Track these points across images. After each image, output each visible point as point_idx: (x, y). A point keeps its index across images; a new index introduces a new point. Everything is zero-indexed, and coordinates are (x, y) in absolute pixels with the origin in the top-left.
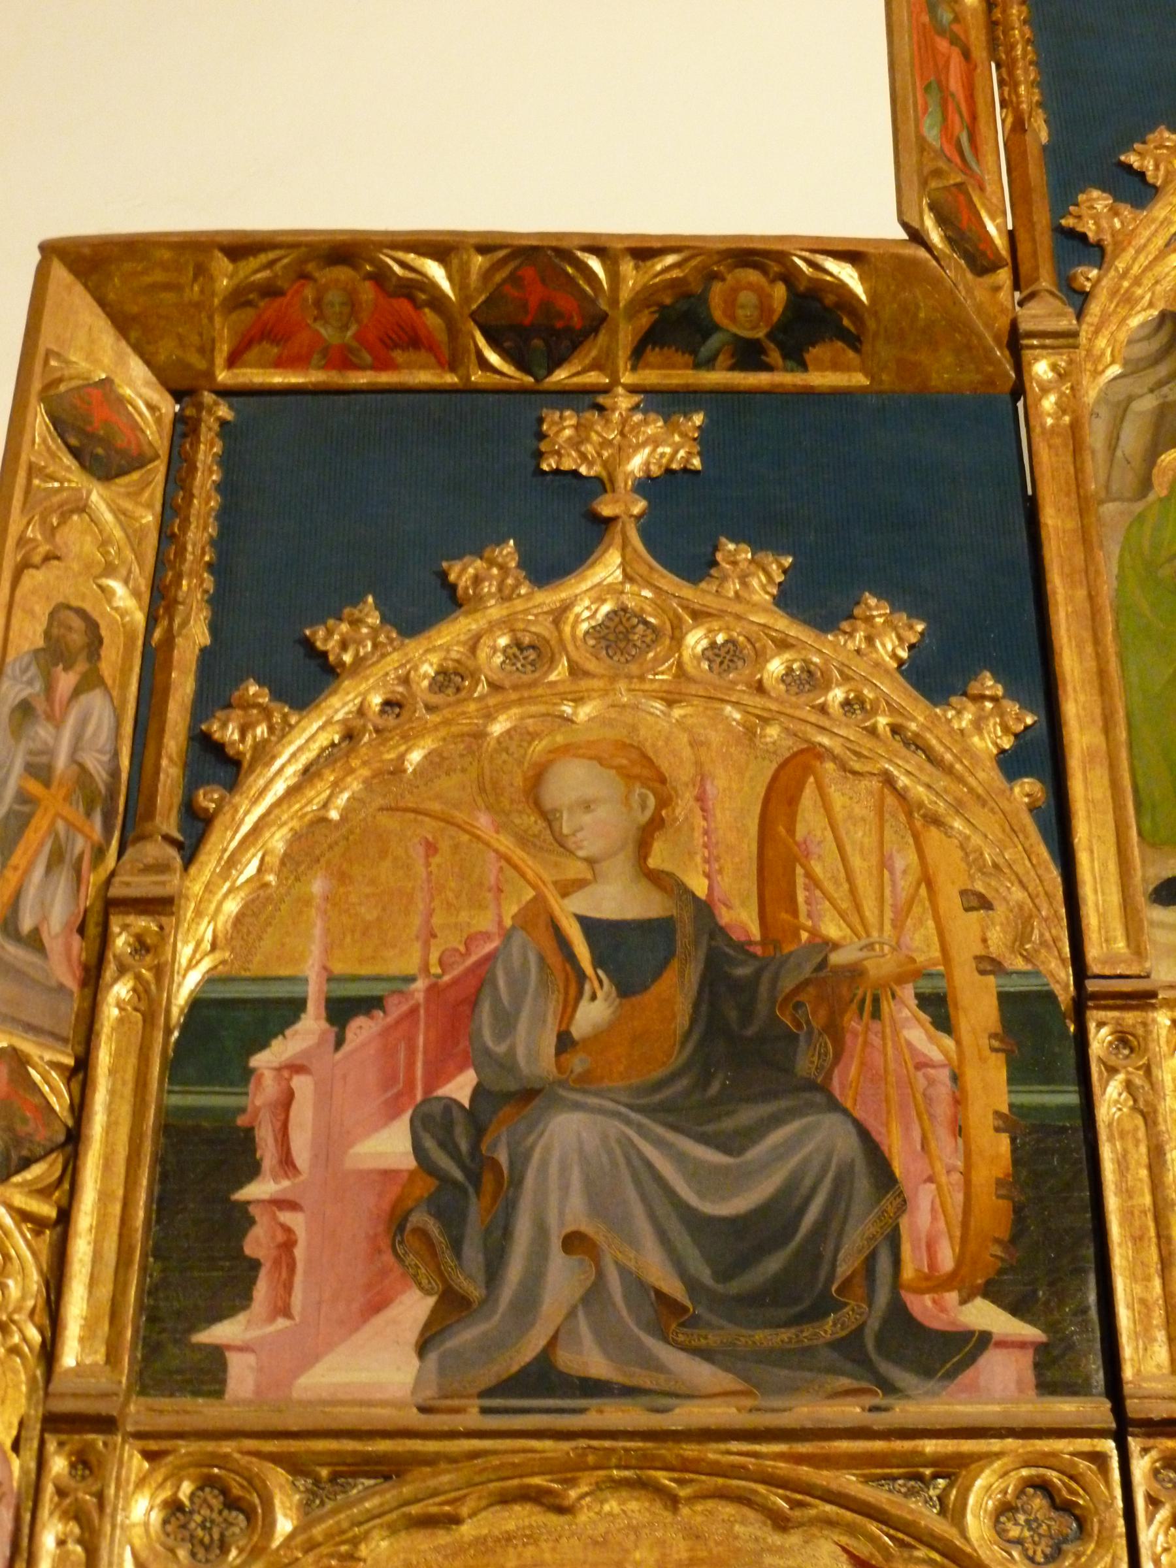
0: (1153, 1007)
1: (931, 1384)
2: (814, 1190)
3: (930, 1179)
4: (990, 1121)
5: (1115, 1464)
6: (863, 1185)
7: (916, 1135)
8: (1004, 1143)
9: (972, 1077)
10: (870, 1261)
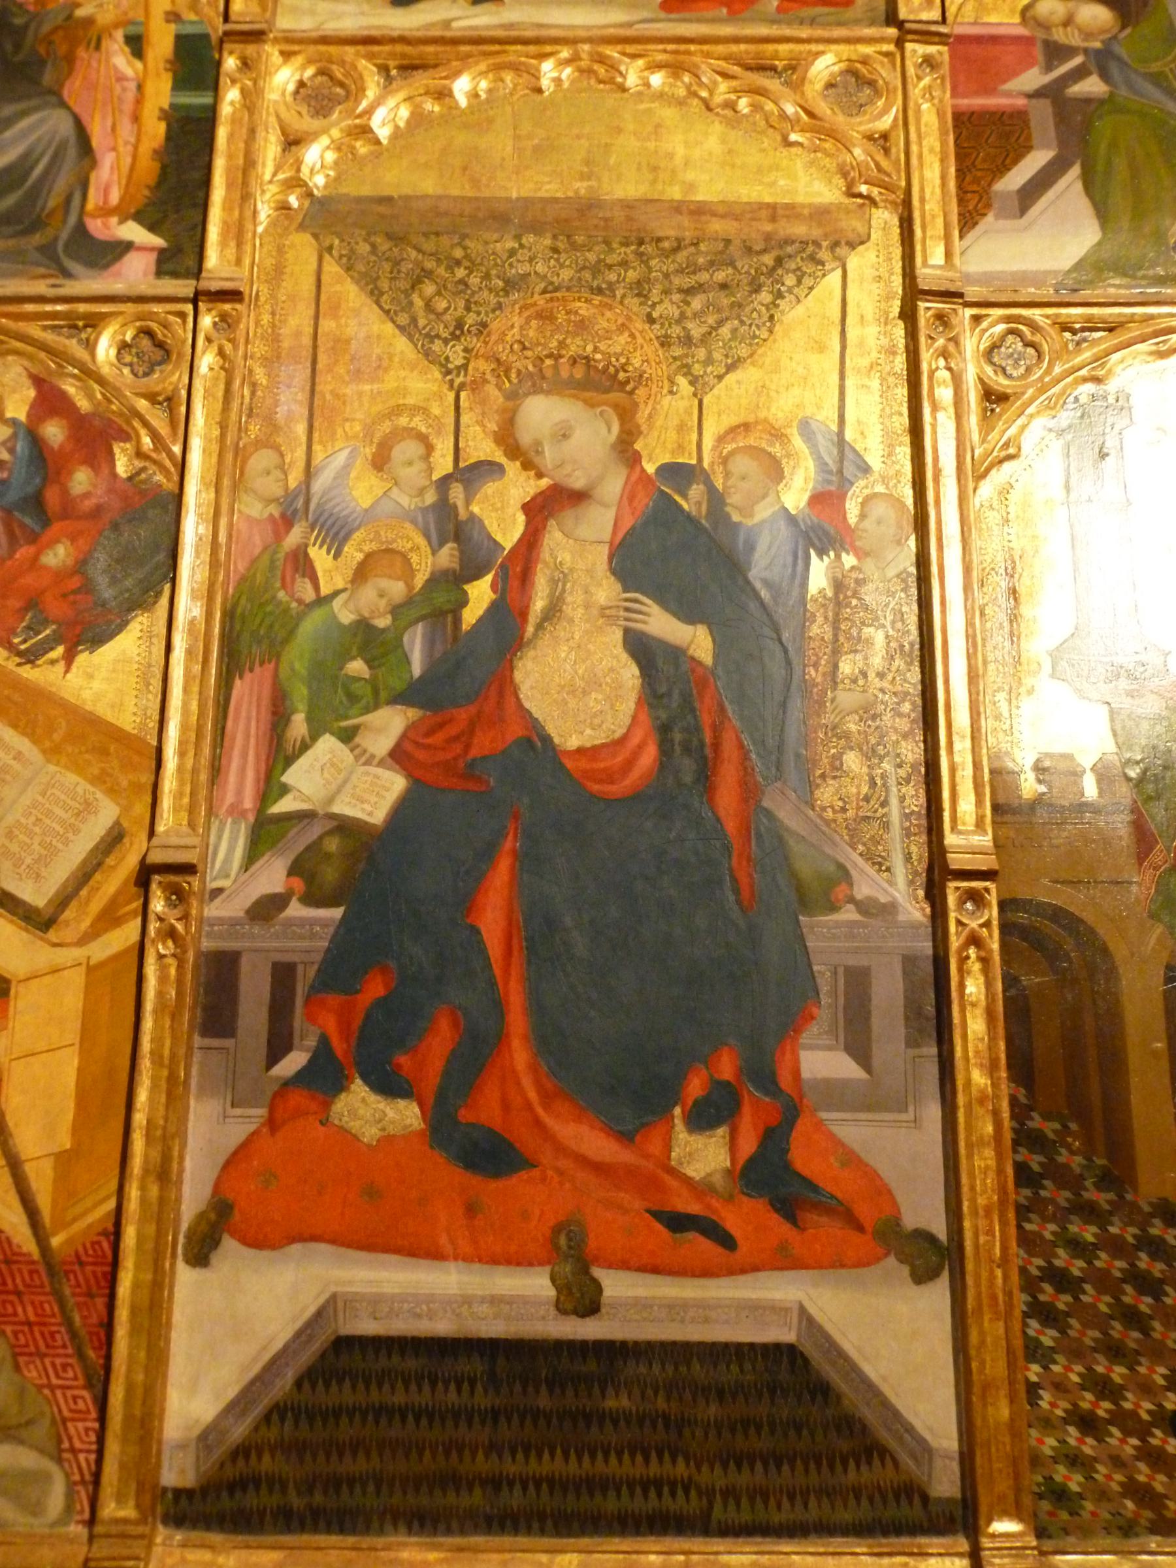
0: (265, 42)
1: (91, 272)
2: (42, 154)
3: (114, 149)
4: (157, 113)
5: (190, 319)
6: (72, 152)
7: (109, 123)
8: (162, 127)
9: (150, 88)
10: (68, 200)
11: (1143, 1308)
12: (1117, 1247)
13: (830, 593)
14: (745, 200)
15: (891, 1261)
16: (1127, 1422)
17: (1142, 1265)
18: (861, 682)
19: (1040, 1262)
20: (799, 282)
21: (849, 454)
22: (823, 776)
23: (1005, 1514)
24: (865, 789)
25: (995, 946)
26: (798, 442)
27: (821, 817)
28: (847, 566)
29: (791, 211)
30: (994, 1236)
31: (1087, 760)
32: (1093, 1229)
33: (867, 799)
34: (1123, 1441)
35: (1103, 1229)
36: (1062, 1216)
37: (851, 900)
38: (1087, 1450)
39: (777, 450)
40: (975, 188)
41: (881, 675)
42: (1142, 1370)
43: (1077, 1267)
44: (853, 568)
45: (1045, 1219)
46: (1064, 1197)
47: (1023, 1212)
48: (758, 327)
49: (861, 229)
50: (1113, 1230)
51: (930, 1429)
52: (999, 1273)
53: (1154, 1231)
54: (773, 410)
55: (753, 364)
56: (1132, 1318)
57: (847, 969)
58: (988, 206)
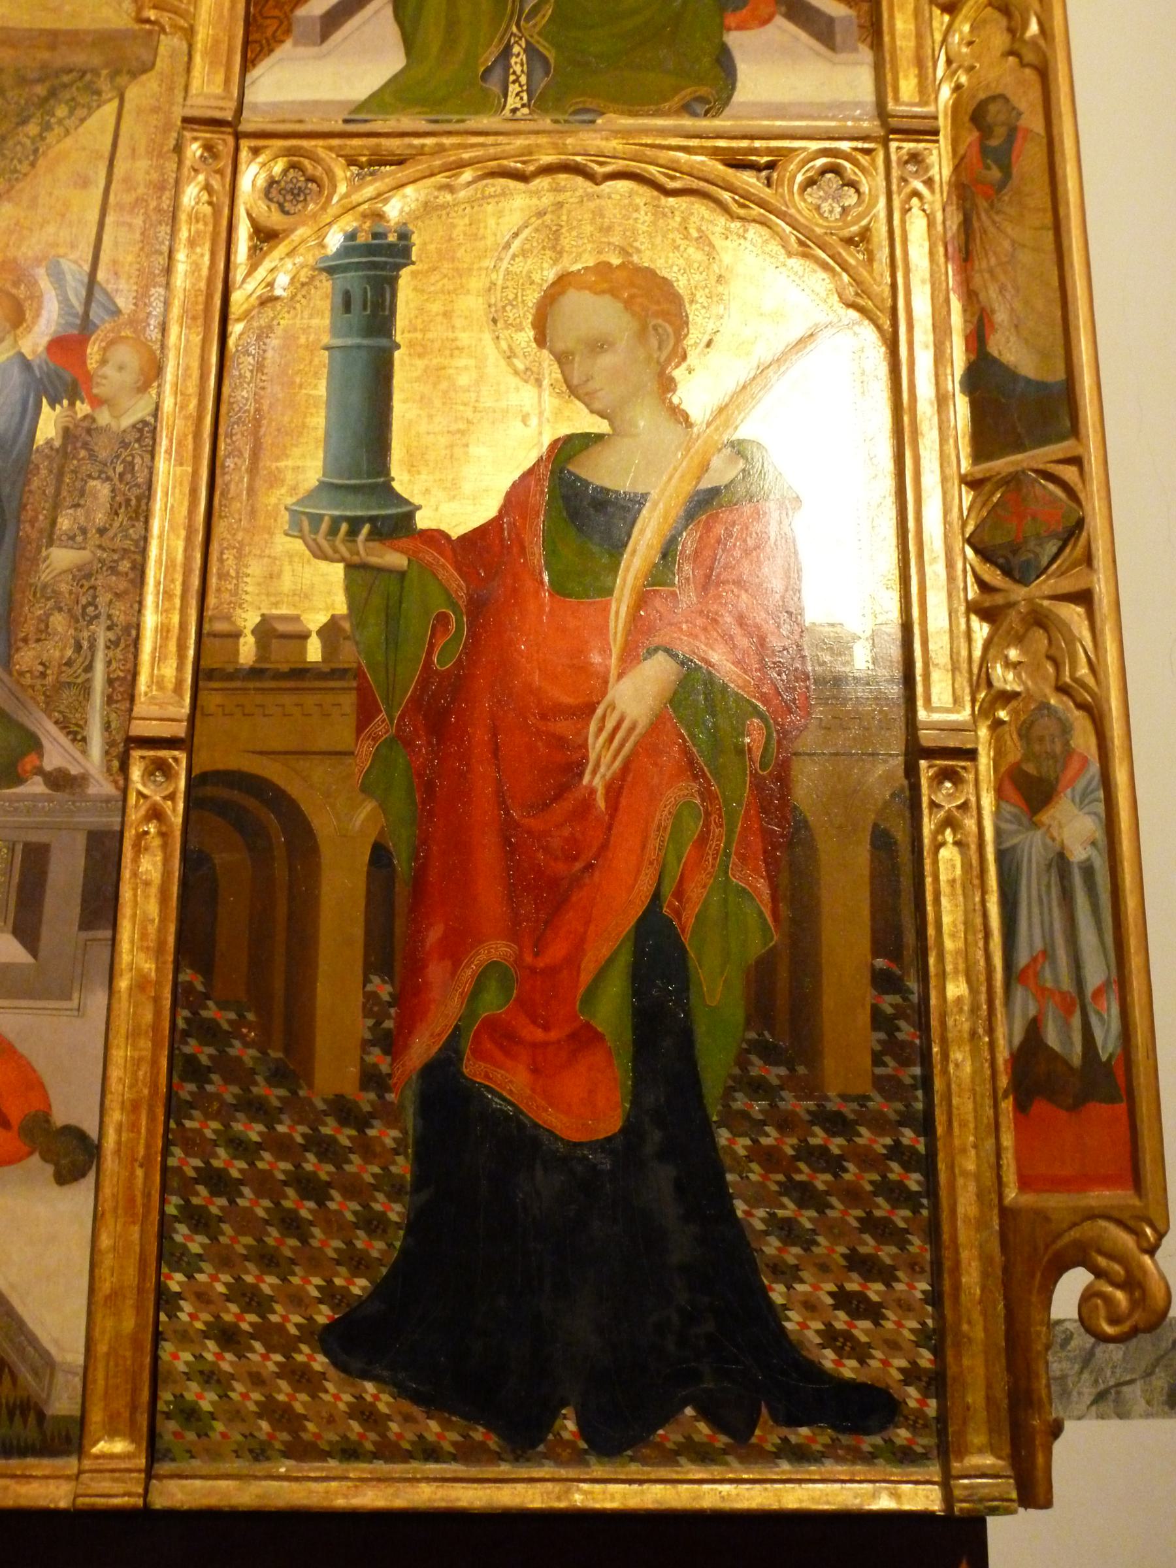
11: (304, 1213)
12: (283, 1147)
13: (57, 444)
14: (27, 26)
15: (36, 1158)
16: (272, 1336)
17: (308, 1167)
18: (79, 539)
19: (197, 1162)
20: (71, 112)
21: (98, 295)
22: (25, 640)
23: (112, 1433)
24: (69, 652)
25: (177, 820)
26: (45, 284)
27: (18, 682)
28: (80, 415)
29: (74, 38)
30: (139, 1132)
31: (315, 620)
32: (260, 1127)
33: (69, 663)
34: (265, 1357)
35: (271, 1128)
36: (225, 1113)
37: (40, 771)
38: (225, 1366)
39: (21, 292)
40: (276, 13)
41: (102, 531)
42: (296, 1280)
43: (237, 1168)
44: (86, 417)
45: (208, 1116)
46: (231, 1093)
47: (174, 1108)
48: (20, 161)
49: (146, 56)
50: (281, 1129)
51: (56, 1342)
52: (140, 1173)
53: (326, 1130)
54: (24, 249)
55: (9, 200)
56: (291, 1224)
57: (26, 845)
58: (288, 32)
